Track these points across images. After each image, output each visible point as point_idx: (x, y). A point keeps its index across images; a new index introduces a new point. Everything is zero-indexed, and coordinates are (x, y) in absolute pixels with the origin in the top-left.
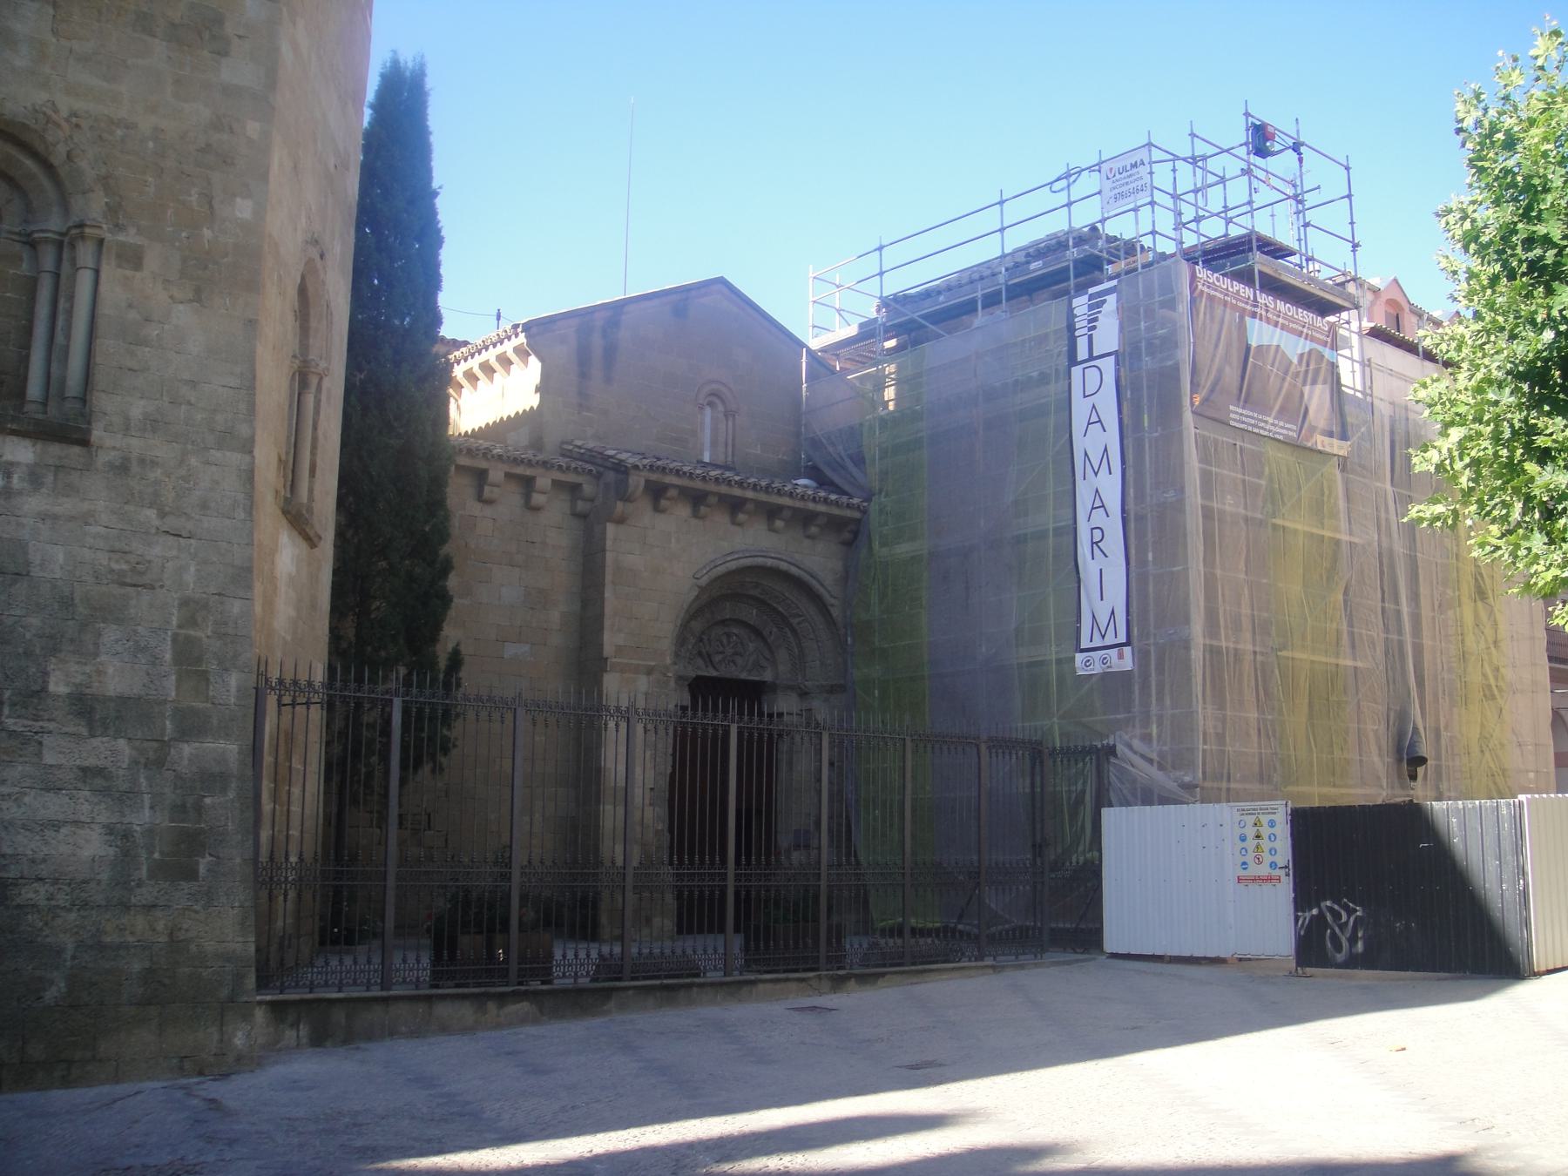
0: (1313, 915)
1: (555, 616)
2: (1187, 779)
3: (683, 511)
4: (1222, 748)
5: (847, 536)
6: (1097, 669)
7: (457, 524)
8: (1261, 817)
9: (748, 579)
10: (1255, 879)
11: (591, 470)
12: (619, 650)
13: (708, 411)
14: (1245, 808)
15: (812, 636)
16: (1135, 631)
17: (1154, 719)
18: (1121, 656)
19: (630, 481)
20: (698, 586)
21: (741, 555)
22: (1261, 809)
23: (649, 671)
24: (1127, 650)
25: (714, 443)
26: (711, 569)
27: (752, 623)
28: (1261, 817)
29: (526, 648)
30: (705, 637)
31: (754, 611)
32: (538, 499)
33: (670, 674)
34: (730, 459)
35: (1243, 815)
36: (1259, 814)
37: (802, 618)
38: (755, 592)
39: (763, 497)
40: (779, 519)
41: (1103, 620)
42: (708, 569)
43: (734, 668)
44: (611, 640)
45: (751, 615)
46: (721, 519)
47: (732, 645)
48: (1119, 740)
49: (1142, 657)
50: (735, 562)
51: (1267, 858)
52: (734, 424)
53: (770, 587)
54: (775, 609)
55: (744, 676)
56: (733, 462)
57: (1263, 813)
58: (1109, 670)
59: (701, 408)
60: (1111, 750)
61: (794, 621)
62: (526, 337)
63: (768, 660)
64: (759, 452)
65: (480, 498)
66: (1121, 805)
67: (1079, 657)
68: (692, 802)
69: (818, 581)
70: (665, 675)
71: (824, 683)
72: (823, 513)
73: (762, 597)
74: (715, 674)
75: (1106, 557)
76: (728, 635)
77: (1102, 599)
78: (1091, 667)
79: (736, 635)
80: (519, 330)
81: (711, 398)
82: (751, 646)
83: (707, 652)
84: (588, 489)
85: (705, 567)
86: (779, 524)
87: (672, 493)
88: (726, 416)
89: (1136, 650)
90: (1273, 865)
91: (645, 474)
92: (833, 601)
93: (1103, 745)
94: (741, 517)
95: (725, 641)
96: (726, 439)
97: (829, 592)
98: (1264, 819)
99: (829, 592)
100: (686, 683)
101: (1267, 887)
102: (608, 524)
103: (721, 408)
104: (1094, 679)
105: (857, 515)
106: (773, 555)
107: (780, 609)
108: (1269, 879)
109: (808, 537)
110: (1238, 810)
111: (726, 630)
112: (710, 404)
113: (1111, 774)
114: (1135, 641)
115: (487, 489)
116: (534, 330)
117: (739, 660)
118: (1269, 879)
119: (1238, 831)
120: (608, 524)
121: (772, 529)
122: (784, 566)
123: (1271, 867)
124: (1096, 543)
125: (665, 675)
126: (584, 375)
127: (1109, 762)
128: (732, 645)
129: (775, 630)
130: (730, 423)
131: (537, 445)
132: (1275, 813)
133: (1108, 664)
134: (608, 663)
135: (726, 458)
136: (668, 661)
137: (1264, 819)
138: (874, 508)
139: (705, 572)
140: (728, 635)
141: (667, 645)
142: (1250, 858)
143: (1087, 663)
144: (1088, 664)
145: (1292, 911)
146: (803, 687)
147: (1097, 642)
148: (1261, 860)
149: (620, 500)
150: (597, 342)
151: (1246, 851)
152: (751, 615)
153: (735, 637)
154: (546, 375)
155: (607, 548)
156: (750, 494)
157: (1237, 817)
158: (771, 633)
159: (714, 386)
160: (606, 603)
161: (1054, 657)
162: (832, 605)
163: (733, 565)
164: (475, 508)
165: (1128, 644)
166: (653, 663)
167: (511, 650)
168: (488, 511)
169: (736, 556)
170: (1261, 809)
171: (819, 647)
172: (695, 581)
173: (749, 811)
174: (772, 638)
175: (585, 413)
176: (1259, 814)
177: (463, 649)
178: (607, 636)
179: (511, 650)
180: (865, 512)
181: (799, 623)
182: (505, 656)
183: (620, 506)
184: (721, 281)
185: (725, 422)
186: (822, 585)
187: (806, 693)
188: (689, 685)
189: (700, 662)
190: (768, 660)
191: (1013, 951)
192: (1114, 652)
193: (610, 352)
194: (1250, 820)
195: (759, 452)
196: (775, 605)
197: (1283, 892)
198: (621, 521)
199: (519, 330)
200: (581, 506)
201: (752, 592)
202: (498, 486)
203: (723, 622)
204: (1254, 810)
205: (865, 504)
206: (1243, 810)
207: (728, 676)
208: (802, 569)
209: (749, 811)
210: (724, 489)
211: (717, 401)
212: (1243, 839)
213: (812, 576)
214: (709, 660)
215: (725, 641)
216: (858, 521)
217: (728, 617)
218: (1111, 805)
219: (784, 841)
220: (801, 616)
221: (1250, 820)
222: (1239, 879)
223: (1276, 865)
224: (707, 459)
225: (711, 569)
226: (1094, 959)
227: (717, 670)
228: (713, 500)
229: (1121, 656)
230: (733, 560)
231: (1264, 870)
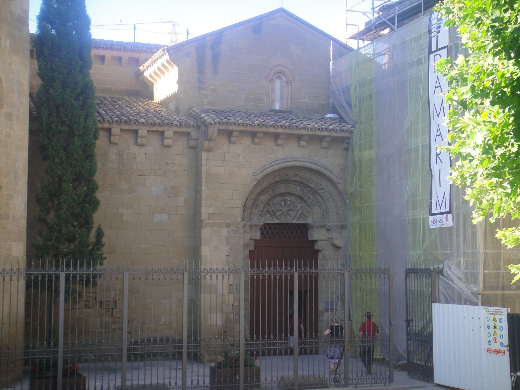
0: (518, 376)
1: (181, 199)
2: (475, 289)
3: (246, 141)
4: (498, 271)
5: (345, 145)
6: (437, 225)
7: (125, 158)
8: (496, 316)
9: (289, 173)
10: (494, 351)
11: (194, 125)
12: (210, 215)
13: (278, 82)
14: (490, 310)
15: (331, 199)
16: (454, 205)
17: (462, 254)
18: (447, 219)
19: (209, 131)
20: (256, 180)
21: (281, 162)
22: (496, 312)
23: (228, 225)
24: (450, 215)
25: (281, 99)
26: (263, 170)
27: (297, 194)
28: (496, 316)
29: (166, 216)
30: (271, 203)
31: (299, 188)
32: (167, 142)
33: (240, 226)
34: (290, 106)
35: (488, 314)
36: (495, 314)
37: (324, 190)
38: (297, 179)
39: (288, 131)
40: (302, 141)
41: (441, 199)
42: (261, 170)
43: (289, 218)
44: (205, 211)
45: (297, 190)
46: (270, 143)
47: (287, 206)
48: (445, 266)
49: (456, 220)
50: (278, 165)
51: (499, 340)
52: (291, 88)
53: (304, 175)
54: (309, 186)
55: (295, 221)
56: (291, 108)
57: (497, 314)
58: (443, 226)
59: (272, 81)
60: (440, 272)
61: (321, 192)
62: (169, 55)
63: (309, 212)
64: (307, 101)
65: (136, 144)
66: (448, 302)
67: (431, 218)
68: (264, 290)
69: (330, 172)
70: (237, 227)
71: (338, 224)
72: (328, 136)
73: (301, 180)
74: (277, 221)
75: (442, 163)
76: (285, 201)
77: (440, 187)
78: (435, 224)
79: (289, 201)
80: (166, 51)
81: (277, 75)
82: (299, 206)
83: (272, 211)
84: (194, 134)
85: (259, 170)
86: (303, 143)
87: (235, 134)
88: (287, 83)
89: (454, 215)
90: (502, 344)
91: (218, 126)
92: (339, 181)
93: (434, 269)
94: (280, 142)
95: (283, 204)
96: (288, 96)
97: (336, 177)
98: (498, 317)
99: (336, 177)
100: (259, 228)
101: (499, 356)
102: (203, 152)
103: (284, 79)
104: (436, 231)
105: (348, 135)
106: (300, 160)
107: (312, 186)
108: (500, 352)
109: (323, 148)
110: (486, 311)
111: (283, 198)
112: (278, 77)
113: (440, 284)
114: (454, 211)
115: (139, 139)
116: (171, 51)
117: (292, 214)
118: (500, 352)
119: (487, 323)
120: (203, 152)
121: (300, 146)
122: (307, 165)
123: (501, 345)
124: (438, 155)
125: (237, 227)
126: (201, 71)
127: (439, 278)
128: (287, 206)
129: (311, 197)
130: (290, 87)
131: (177, 111)
132: (502, 315)
133: (442, 223)
134: (203, 223)
135: (288, 105)
136: (239, 219)
137: (498, 317)
138: (355, 131)
139: (259, 172)
140: (285, 201)
141: (238, 211)
142: (492, 339)
143: (434, 222)
144: (434, 222)
145: (510, 372)
146: (328, 227)
147: (438, 211)
148: (496, 341)
149: (206, 140)
150: (208, 54)
151: (490, 335)
152: (297, 190)
153: (288, 202)
154: (180, 75)
155: (203, 164)
156: (280, 131)
157: (486, 315)
158: (309, 198)
159: (279, 68)
160: (203, 192)
161: (421, 217)
162: (339, 183)
163: (276, 167)
164: (135, 149)
165: (449, 212)
166: (229, 222)
167: (157, 218)
168: (142, 150)
169: (278, 162)
170: (496, 312)
171: (335, 205)
172: (254, 177)
173: (306, 292)
174: (310, 201)
175: (202, 92)
176: (495, 314)
177: (103, 228)
178: (203, 210)
179: (157, 218)
180: (351, 133)
181: (323, 193)
182: (154, 221)
183: (206, 143)
184: (282, 10)
185: (287, 87)
186: (332, 173)
187: (330, 230)
188: (261, 229)
189: (268, 216)
190: (309, 212)
191: (418, 375)
192: (444, 216)
193: (216, 58)
194: (492, 317)
195: (307, 101)
196: (309, 184)
197: (505, 360)
198: (209, 150)
199: (166, 51)
200: (192, 143)
201: (294, 179)
202: (145, 137)
203: (281, 194)
204: (493, 312)
205: (352, 129)
206: (488, 311)
207: (285, 222)
208: (319, 166)
209: (306, 292)
210: (264, 129)
211: (281, 75)
212: (489, 328)
213: (325, 169)
214: (273, 214)
215: (283, 204)
216: (349, 138)
217: (283, 192)
218: (439, 302)
219: (321, 306)
220: (323, 189)
221: (492, 317)
222: (488, 350)
223: (503, 344)
224: (277, 106)
225: (263, 170)
226: (425, 386)
227: (279, 220)
228: (261, 135)
229: (447, 219)
230: (276, 164)
231: (497, 347)
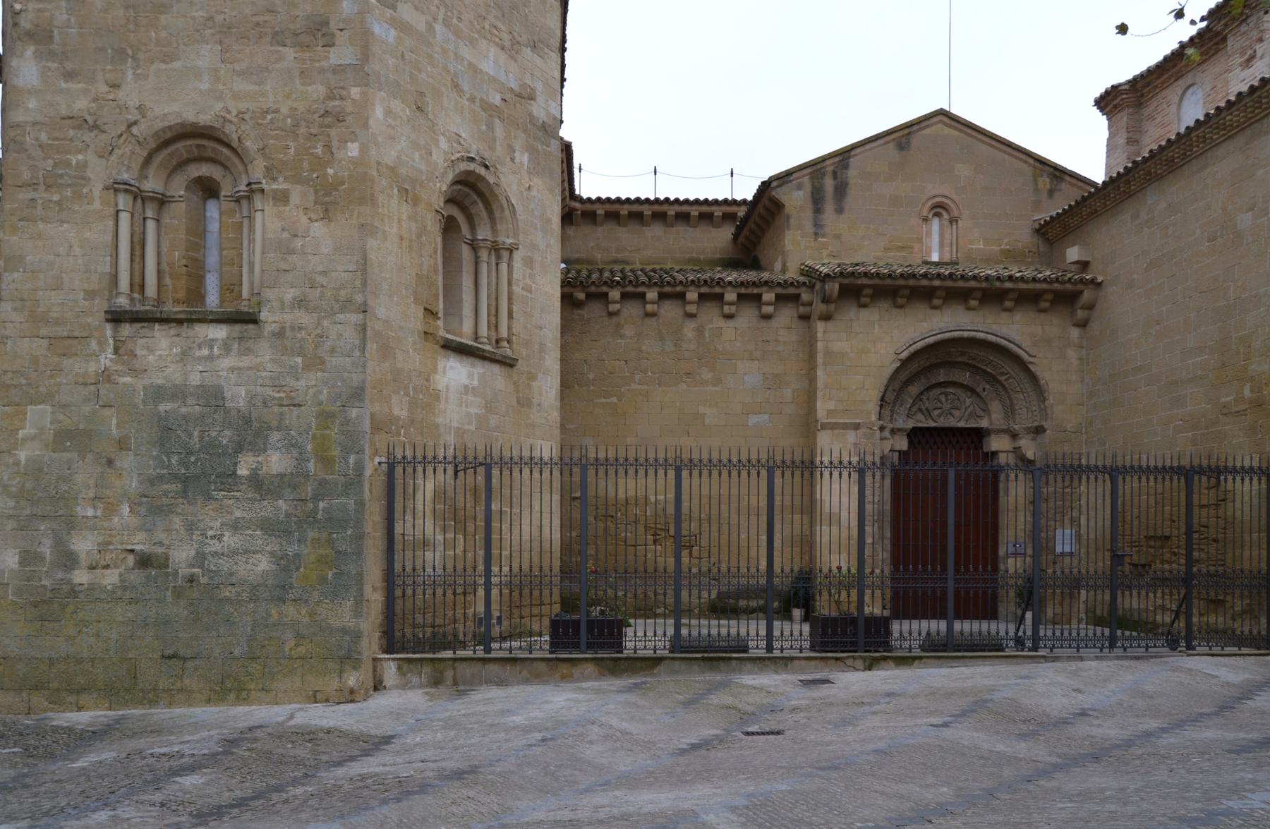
1: (788, 393)
9: (953, 350)
12: (830, 413)
15: (1018, 389)
29: (766, 417)
30: (924, 398)
31: (968, 374)
33: (875, 428)
34: (954, 255)
43: (952, 419)
44: (822, 407)
54: (984, 371)
55: (962, 424)
61: (1002, 378)
64: (982, 247)
74: (933, 424)
103: (946, 216)
107: (988, 370)
111: (943, 390)
112: (937, 215)
117: (957, 413)
121: (969, 309)
136: (874, 418)
141: (872, 407)
158: (984, 390)
166: (858, 421)
168: (731, 323)
178: (819, 404)
181: (1007, 380)
186: (1020, 347)
187: (1016, 435)
189: (920, 416)
195: (982, 247)
201: (960, 359)
203: (940, 385)
207: (946, 425)
210: (912, 282)
214: (928, 413)
224: (935, 257)
227: (936, 422)
